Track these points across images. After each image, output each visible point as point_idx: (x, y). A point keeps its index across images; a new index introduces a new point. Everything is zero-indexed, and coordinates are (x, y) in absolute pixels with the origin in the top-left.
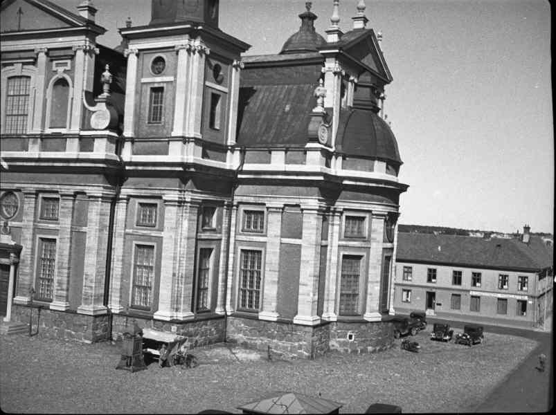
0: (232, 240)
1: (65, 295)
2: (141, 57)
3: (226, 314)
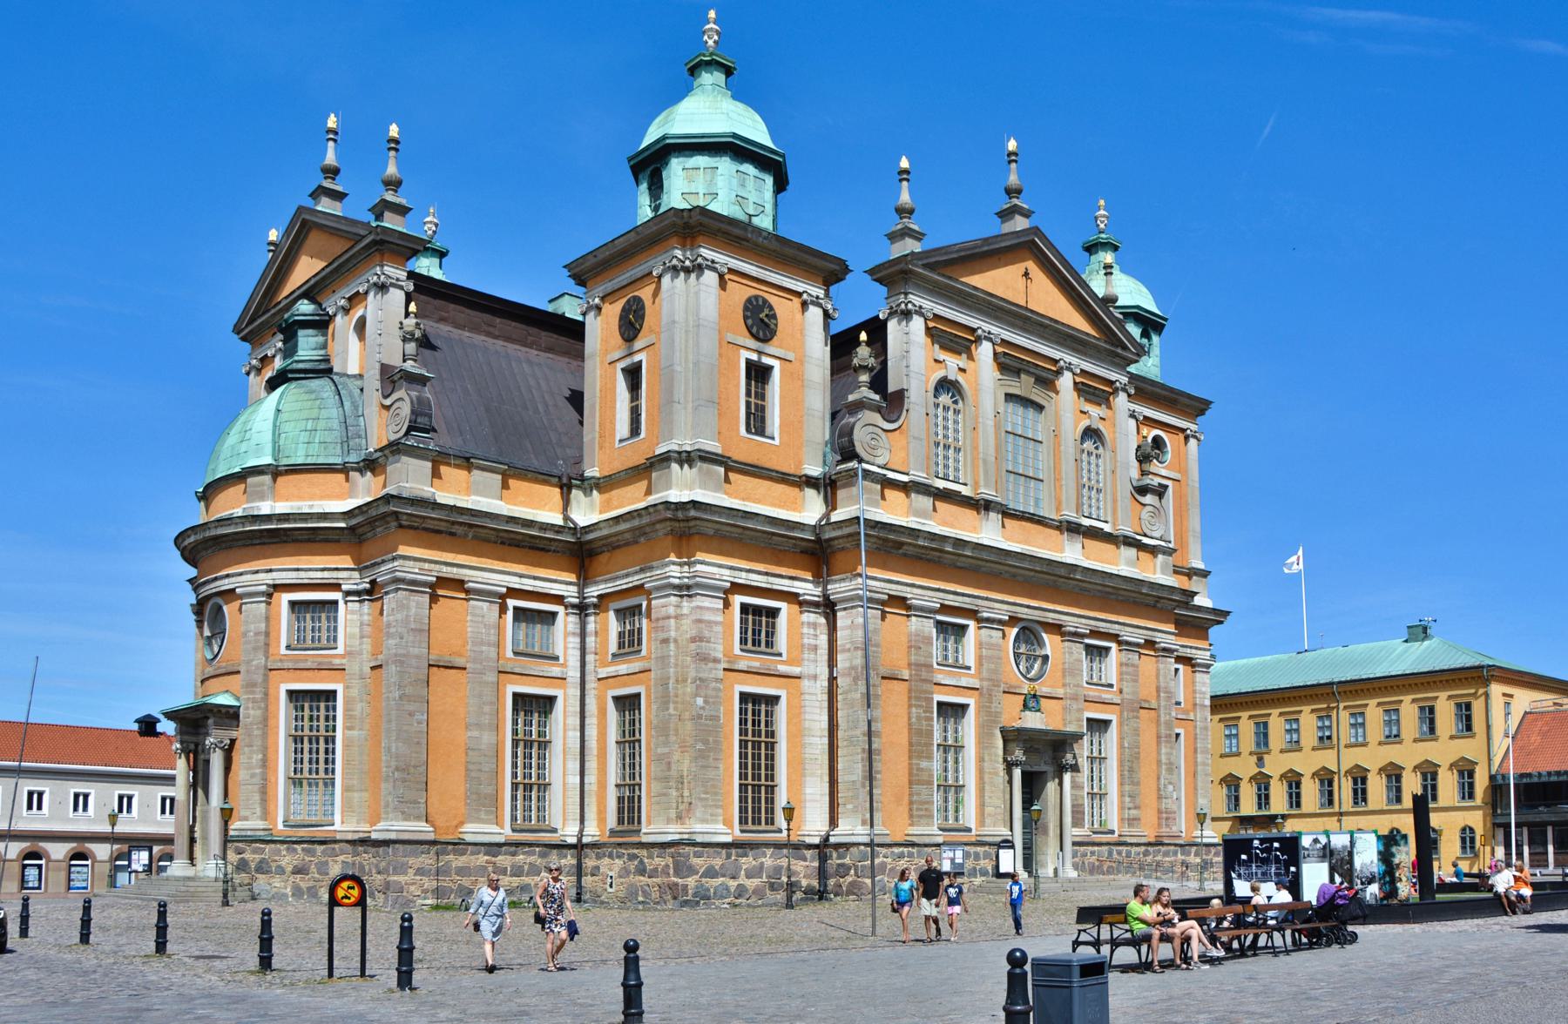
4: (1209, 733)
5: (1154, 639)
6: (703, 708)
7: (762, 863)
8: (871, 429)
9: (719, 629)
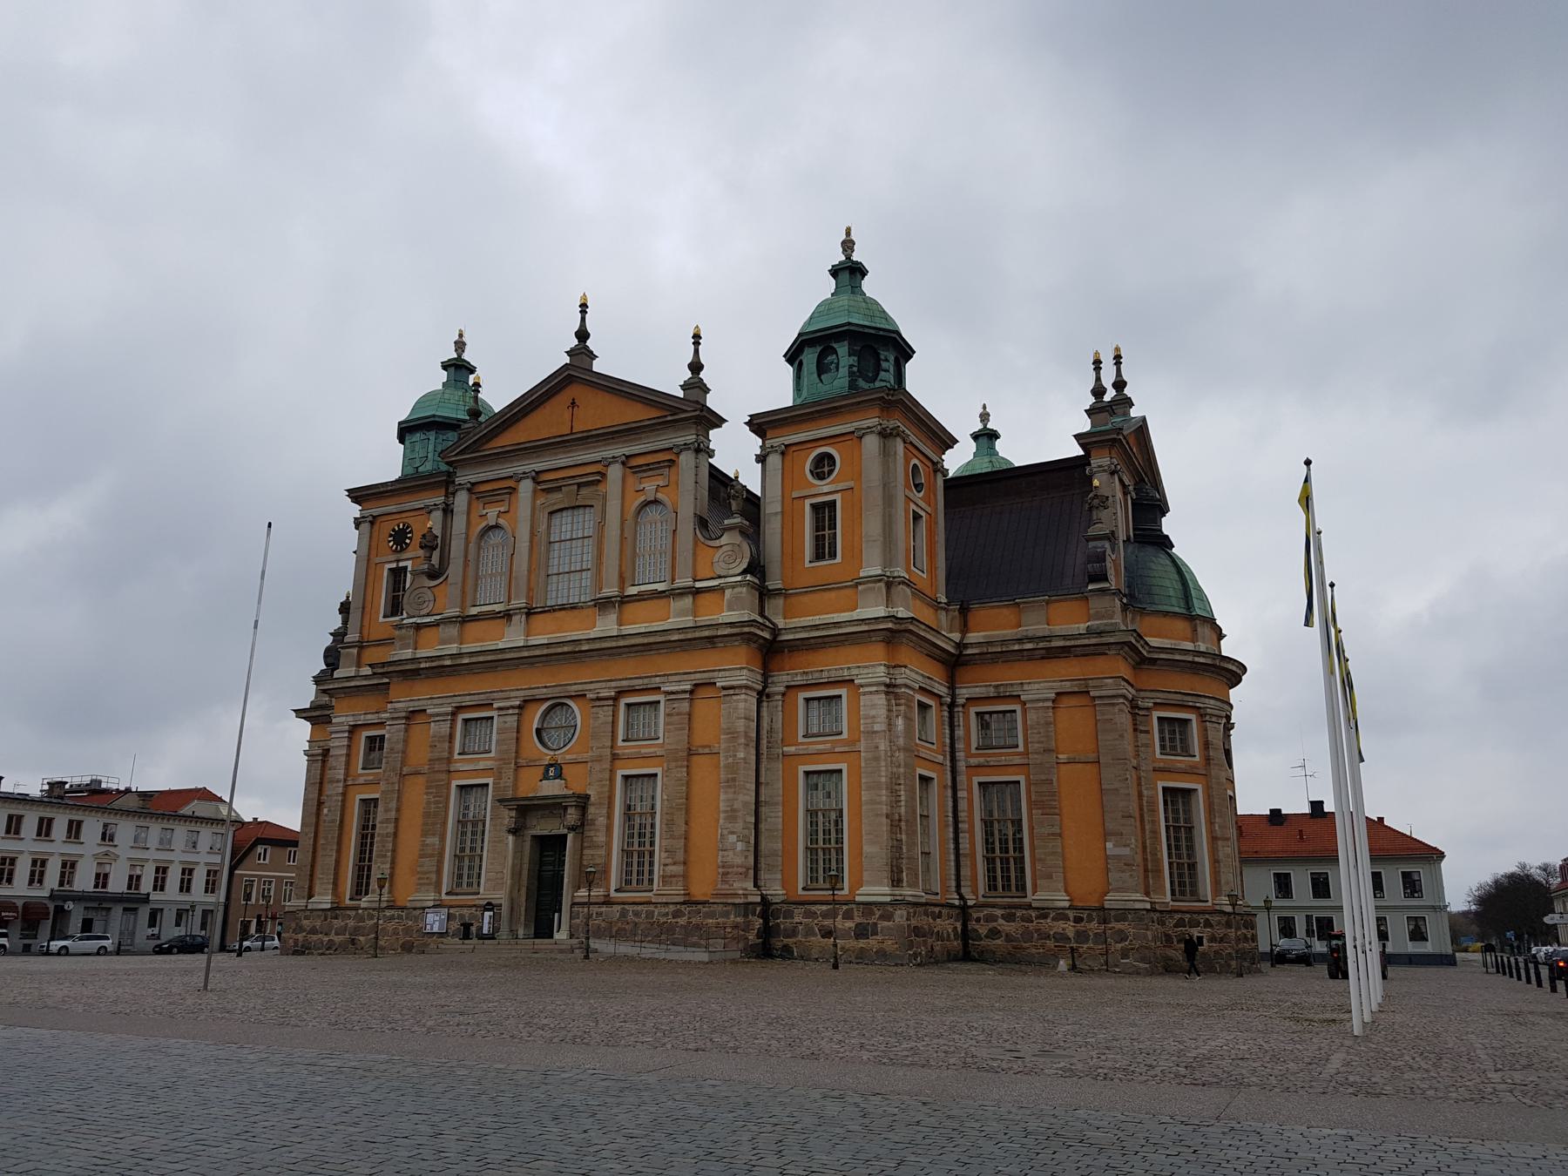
0: (961, 765)
1: (682, 873)
2: (788, 458)
3: (965, 903)
4: (883, 764)
5: (712, 681)
6: (326, 815)
7: (347, 924)
8: (417, 592)
9: (343, 759)
